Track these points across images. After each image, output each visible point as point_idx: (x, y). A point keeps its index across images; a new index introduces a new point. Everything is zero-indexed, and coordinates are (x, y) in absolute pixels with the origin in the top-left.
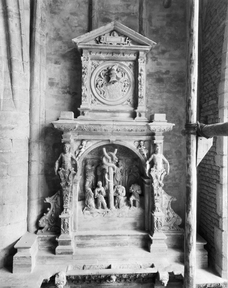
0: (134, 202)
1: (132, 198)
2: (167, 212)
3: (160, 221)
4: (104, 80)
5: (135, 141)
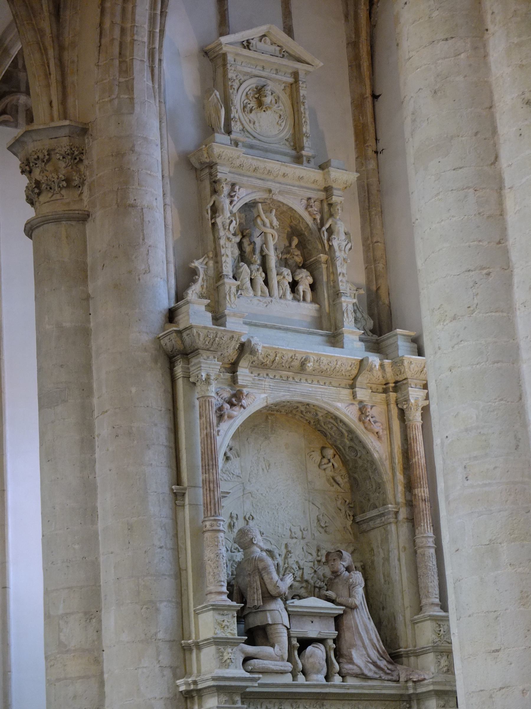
4: (253, 104)
5: (302, 199)
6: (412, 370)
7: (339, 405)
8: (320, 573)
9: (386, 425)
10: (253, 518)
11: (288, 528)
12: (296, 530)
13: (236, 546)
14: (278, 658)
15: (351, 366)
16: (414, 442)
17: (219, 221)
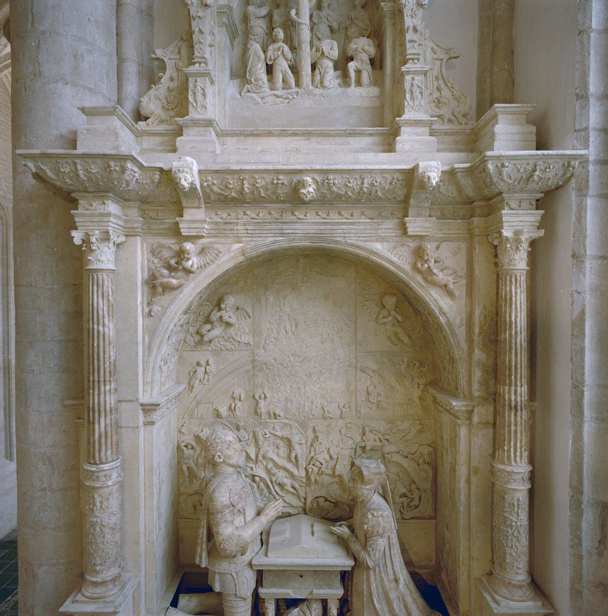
0: (358, 72)
1: (352, 66)
2: (436, 84)
3: (420, 85)
6: (505, 178)
7: (378, 246)
9: (463, 272)
10: (265, 397)
11: (319, 405)
15: (391, 183)
16: (506, 305)
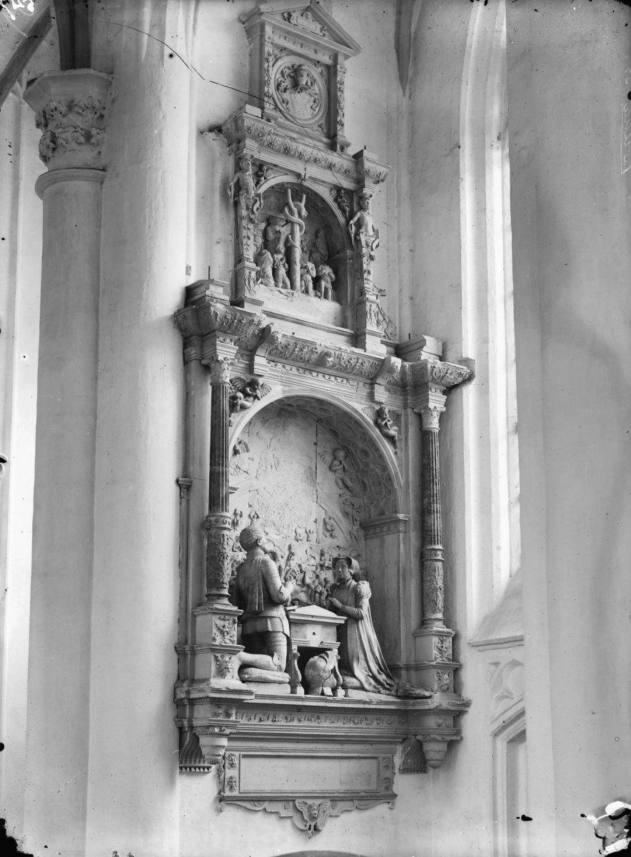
4: (288, 83)
8: (322, 577)
10: (258, 517)
11: (294, 529)
12: (301, 531)
13: (239, 544)
14: (276, 668)
17: (243, 204)
